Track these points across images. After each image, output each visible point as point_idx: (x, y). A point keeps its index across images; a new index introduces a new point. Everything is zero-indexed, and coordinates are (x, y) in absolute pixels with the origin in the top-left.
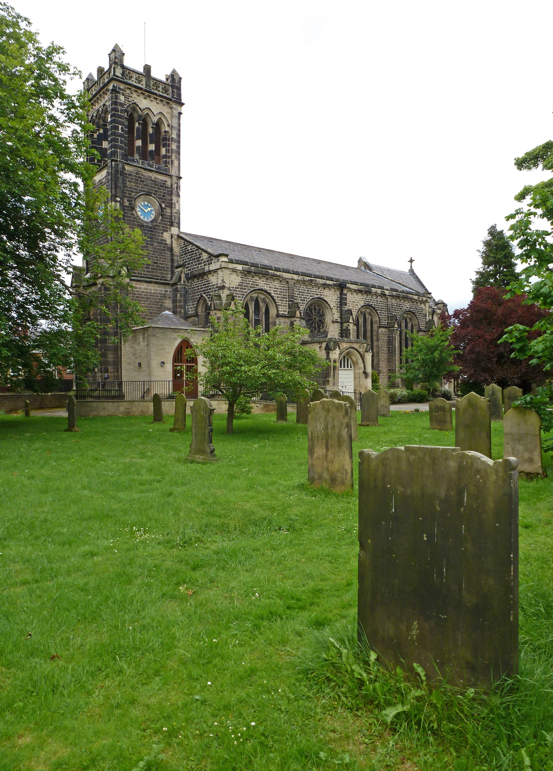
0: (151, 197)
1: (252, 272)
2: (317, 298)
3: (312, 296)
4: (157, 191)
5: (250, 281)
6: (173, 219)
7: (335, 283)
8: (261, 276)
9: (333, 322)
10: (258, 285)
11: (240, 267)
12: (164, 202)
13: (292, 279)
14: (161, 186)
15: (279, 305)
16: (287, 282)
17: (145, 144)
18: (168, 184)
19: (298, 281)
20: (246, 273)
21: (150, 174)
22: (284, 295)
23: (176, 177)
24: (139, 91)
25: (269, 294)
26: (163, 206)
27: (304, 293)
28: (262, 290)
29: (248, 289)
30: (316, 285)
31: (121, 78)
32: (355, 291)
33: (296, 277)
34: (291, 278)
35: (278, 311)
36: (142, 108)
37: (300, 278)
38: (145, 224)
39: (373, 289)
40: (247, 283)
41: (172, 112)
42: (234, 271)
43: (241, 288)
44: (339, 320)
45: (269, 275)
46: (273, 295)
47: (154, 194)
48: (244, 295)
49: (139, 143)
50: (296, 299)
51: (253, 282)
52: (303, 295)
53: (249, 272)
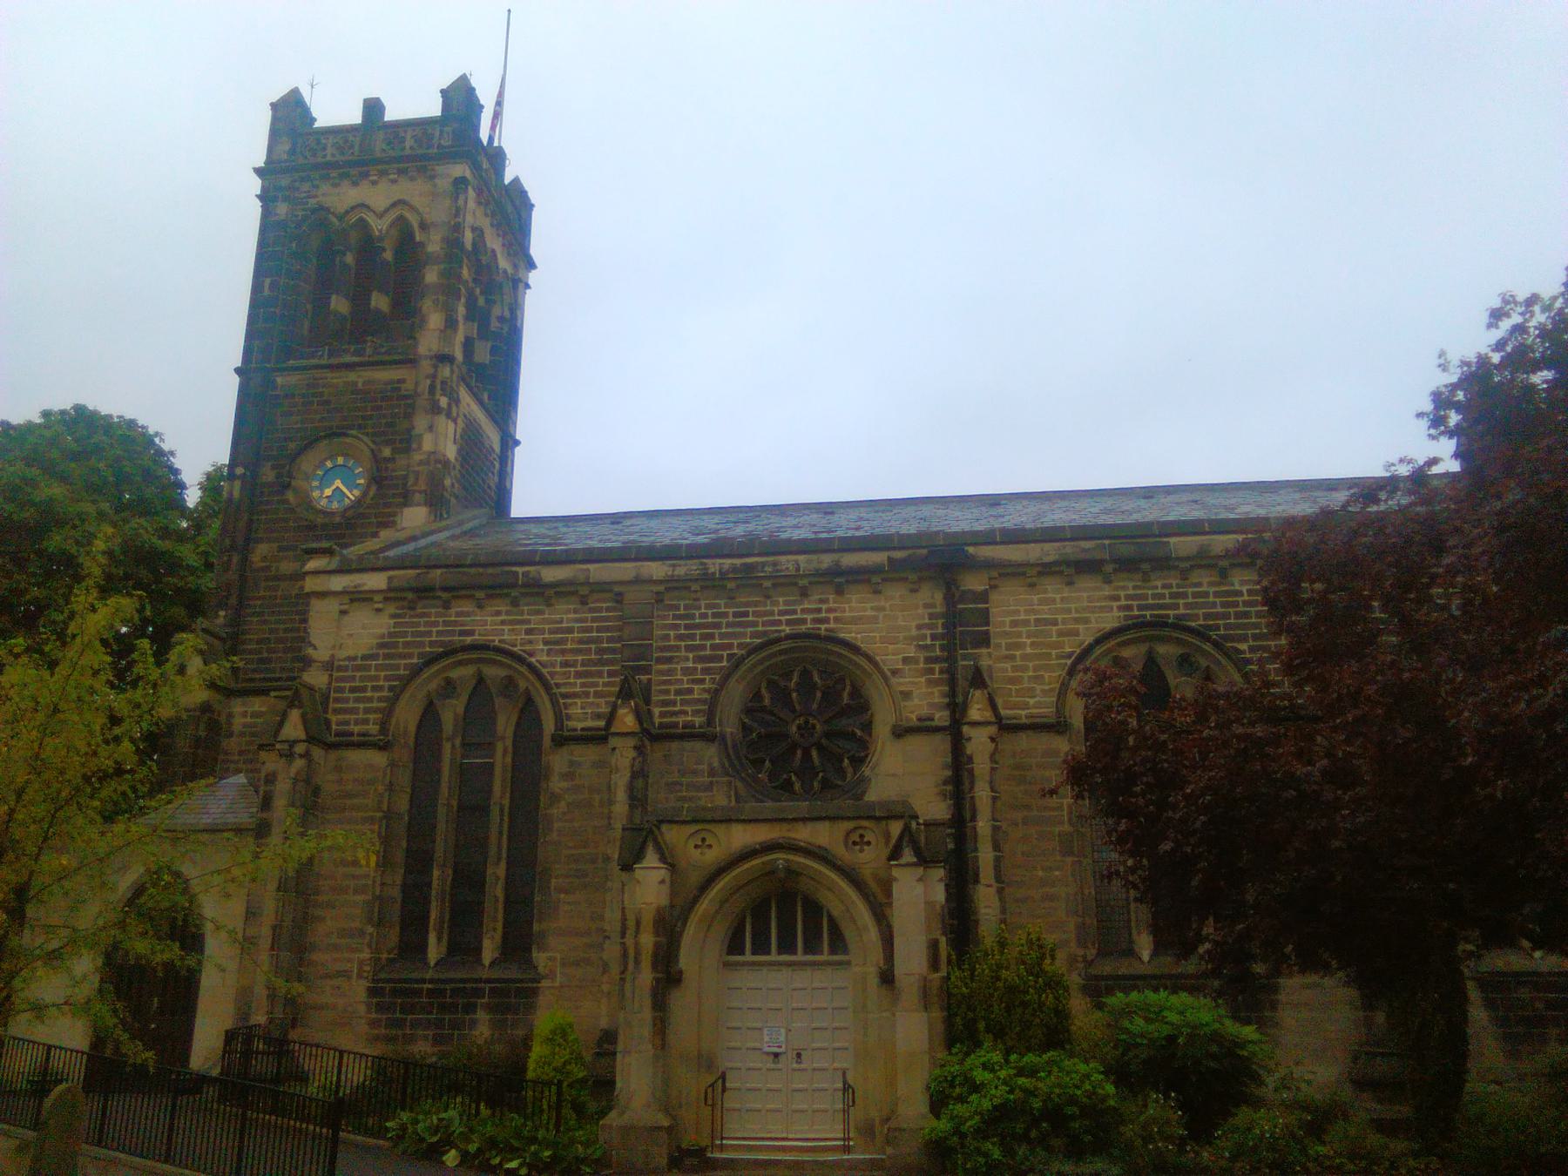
0: (348, 440)
1: (432, 589)
2: (788, 637)
3: (765, 633)
4: (371, 417)
5: (435, 624)
6: (411, 481)
7: (898, 555)
8: (480, 594)
9: (900, 732)
10: (471, 633)
11: (376, 581)
12: (387, 443)
13: (637, 581)
14: (383, 399)
15: (574, 695)
16: (619, 598)
17: (359, 299)
18: (409, 386)
19: (674, 585)
20: (410, 595)
21: (352, 376)
22: (600, 651)
23: (431, 358)
24: (334, 174)
25: (519, 659)
26: (387, 452)
27: (717, 626)
28: (484, 647)
29: (421, 655)
30: (786, 582)
31: (286, 161)
32: (1047, 569)
33: (657, 570)
34: (630, 575)
35: (560, 719)
36: (343, 211)
37: (681, 571)
38: (320, 520)
39: (1173, 540)
40: (414, 634)
41: (435, 186)
42: (357, 597)
43: (386, 656)
44: (942, 718)
45: (514, 586)
46: (541, 657)
47: (360, 427)
48: (399, 678)
49: (339, 304)
50: (669, 660)
51: (446, 623)
52: (712, 636)
53: (424, 592)
